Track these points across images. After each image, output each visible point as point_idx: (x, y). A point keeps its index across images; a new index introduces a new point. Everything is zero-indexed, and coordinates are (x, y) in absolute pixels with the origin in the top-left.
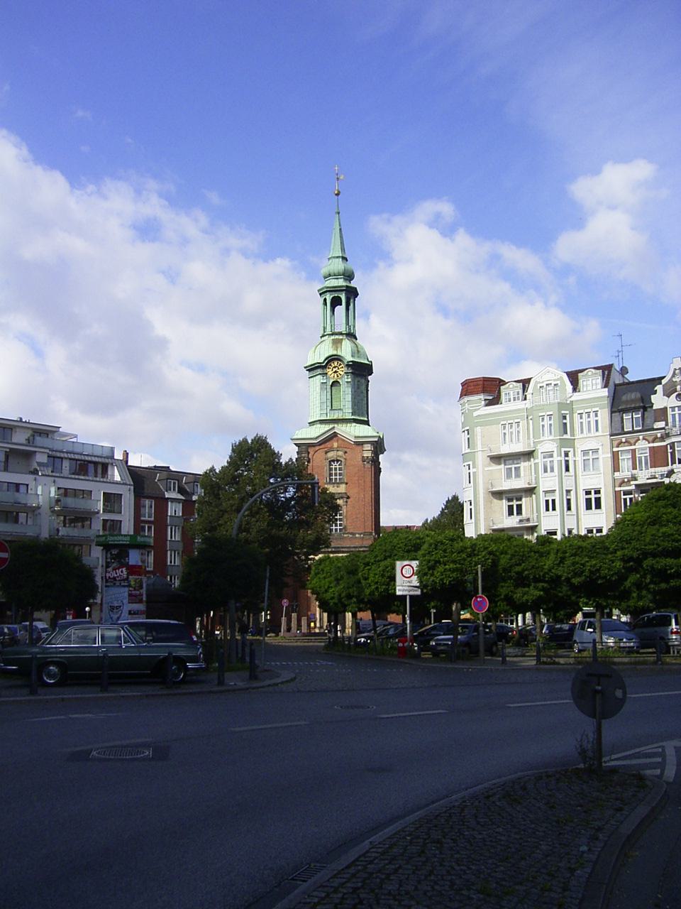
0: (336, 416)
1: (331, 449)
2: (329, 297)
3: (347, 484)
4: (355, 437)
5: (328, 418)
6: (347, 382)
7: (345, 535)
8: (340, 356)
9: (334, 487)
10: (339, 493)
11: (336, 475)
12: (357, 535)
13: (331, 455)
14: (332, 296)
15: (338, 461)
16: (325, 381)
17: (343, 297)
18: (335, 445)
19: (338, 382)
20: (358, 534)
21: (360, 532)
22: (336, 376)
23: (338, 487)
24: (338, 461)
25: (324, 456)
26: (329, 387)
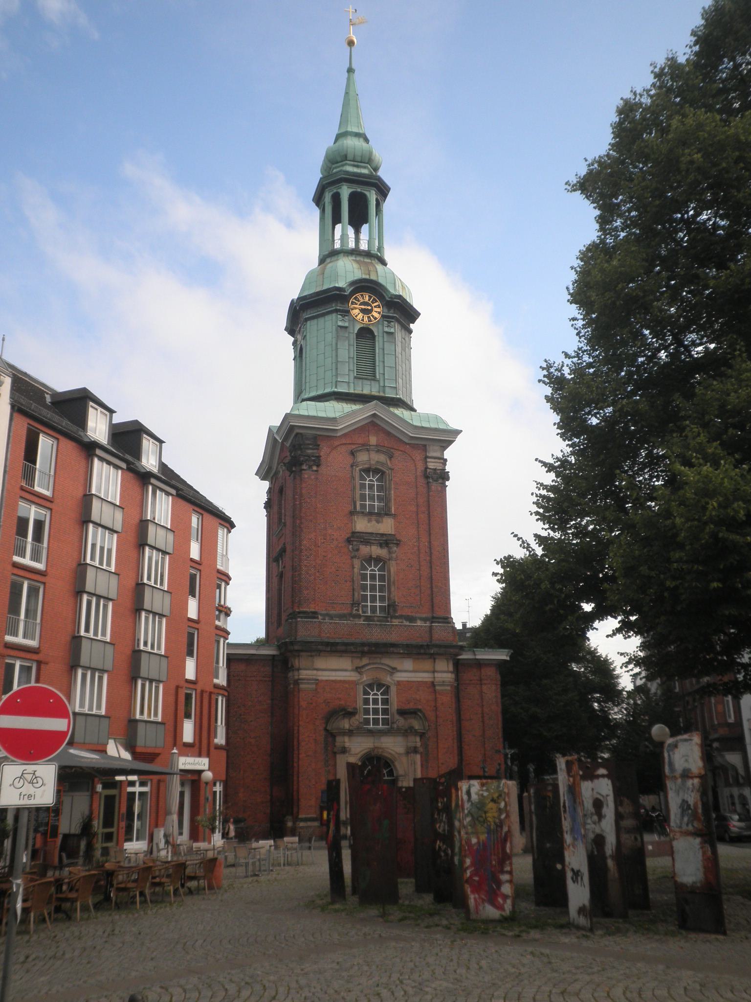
0: (366, 389)
1: (366, 447)
2: (345, 192)
3: (394, 516)
4: (416, 427)
5: (352, 391)
6: (387, 333)
7: (396, 622)
8: (376, 283)
9: (370, 521)
10: (382, 535)
11: (372, 498)
12: (419, 623)
13: (363, 457)
14: (351, 190)
15: (376, 471)
16: (346, 324)
17: (372, 196)
18: (373, 440)
19: (370, 332)
20: (422, 619)
21: (424, 616)
22: (366, 319)
23: (378, 522)
24: (376, 471)
25: (350, 460)
26: (353, 337)
